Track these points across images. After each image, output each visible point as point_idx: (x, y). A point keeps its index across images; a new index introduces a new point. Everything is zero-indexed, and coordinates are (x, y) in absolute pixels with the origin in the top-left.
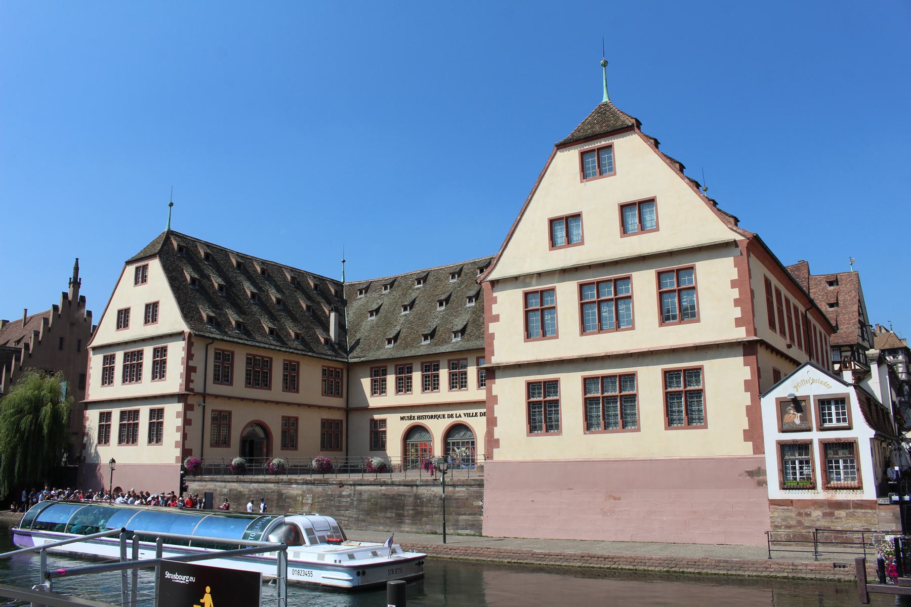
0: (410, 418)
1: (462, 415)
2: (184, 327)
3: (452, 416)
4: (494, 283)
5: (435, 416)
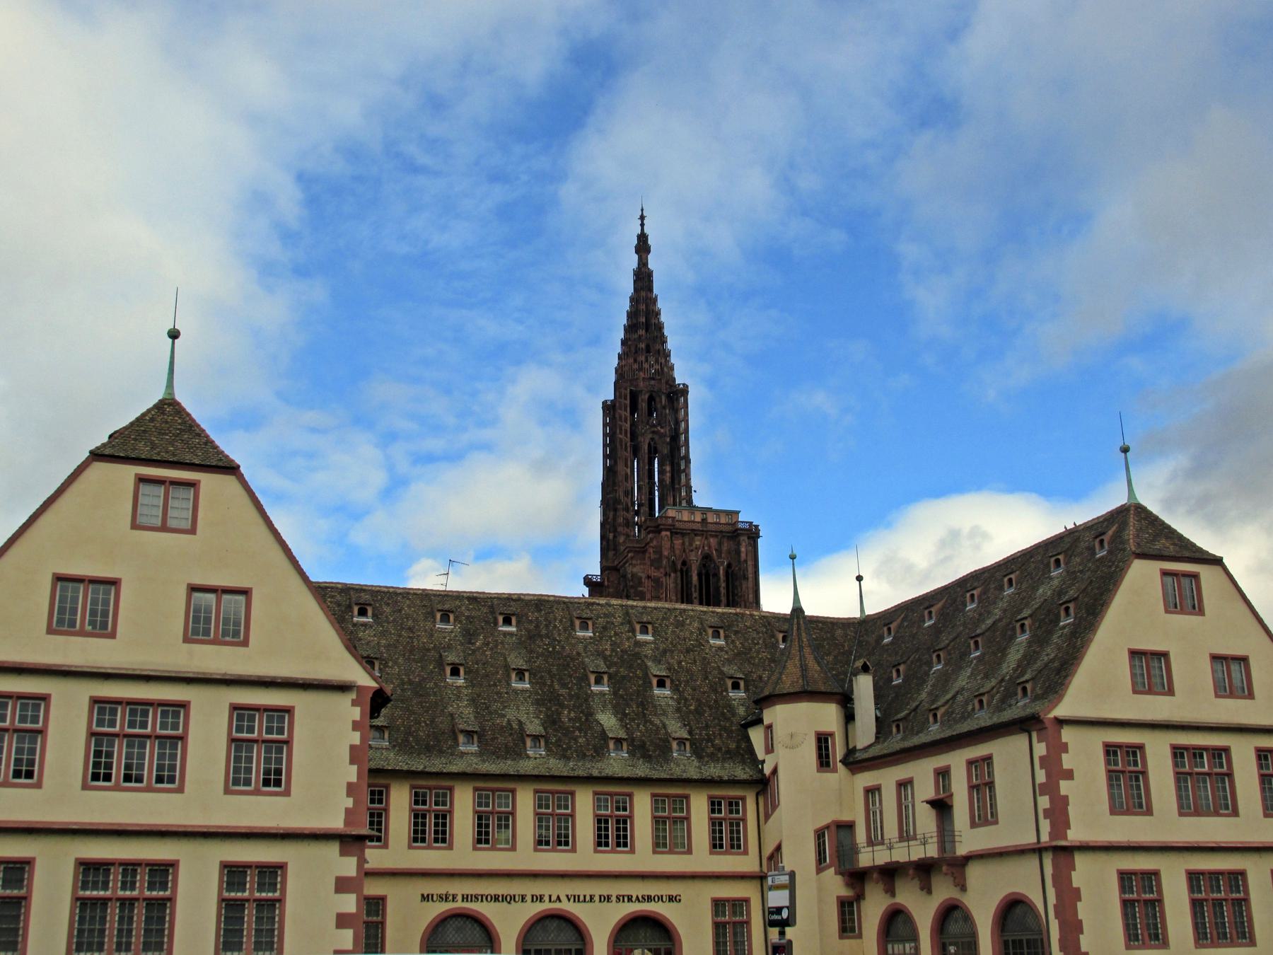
0: (444, 898)
1: (563, 898)
2: (364, 679)
3: (541, 898)
4: (1061, 722)
5: (504, 898)
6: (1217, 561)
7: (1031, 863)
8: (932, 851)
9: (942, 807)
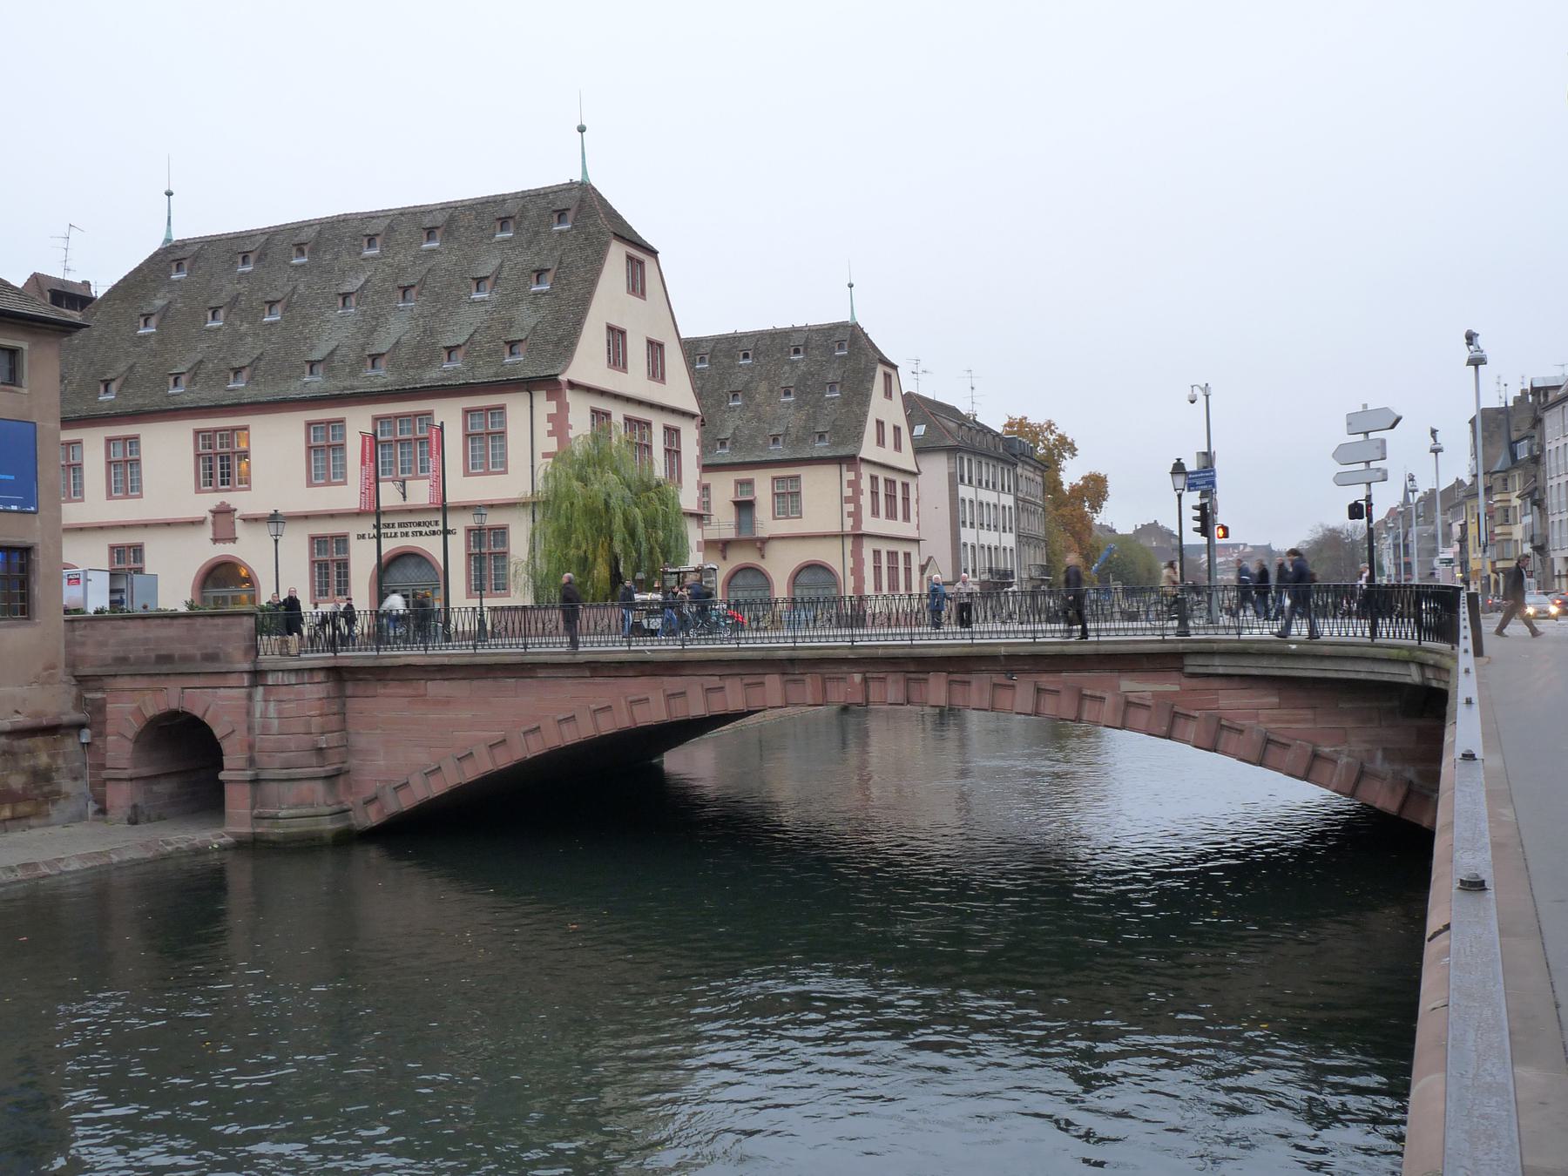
4: (862, 460)
6: (895, 367)
7: (838, 542)
8: (730, 534)
9: (744, 507)
